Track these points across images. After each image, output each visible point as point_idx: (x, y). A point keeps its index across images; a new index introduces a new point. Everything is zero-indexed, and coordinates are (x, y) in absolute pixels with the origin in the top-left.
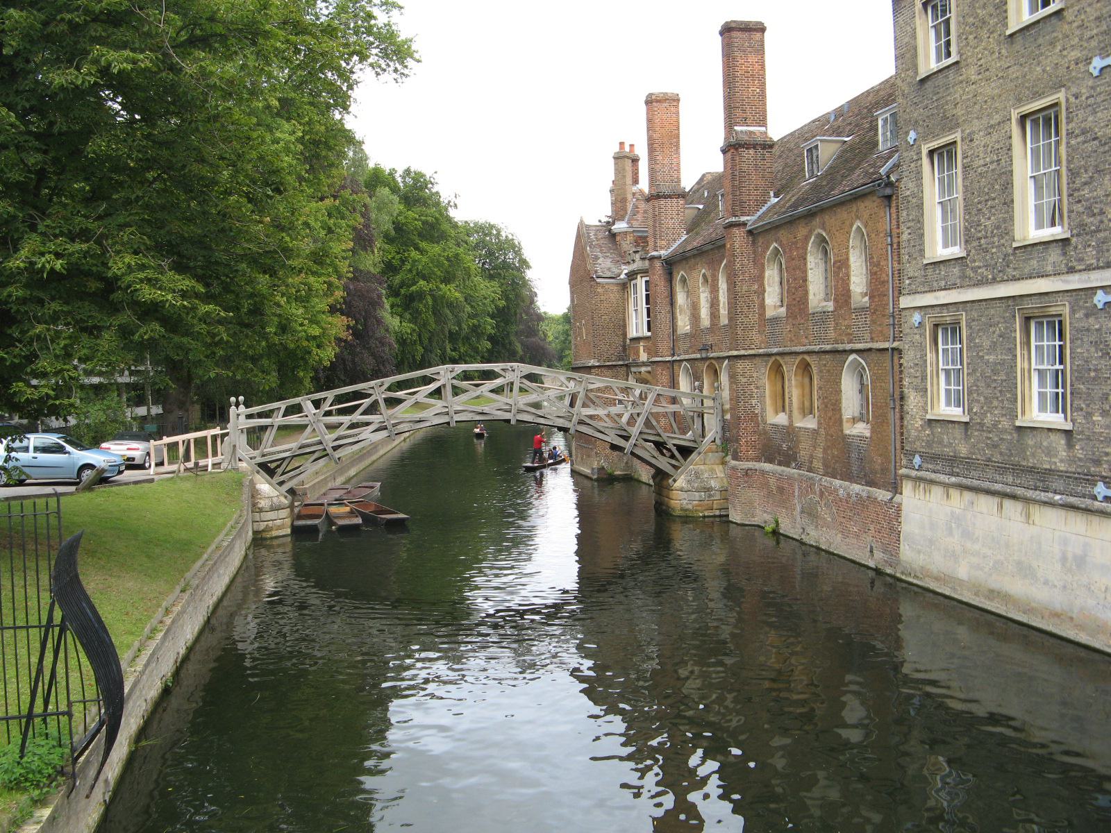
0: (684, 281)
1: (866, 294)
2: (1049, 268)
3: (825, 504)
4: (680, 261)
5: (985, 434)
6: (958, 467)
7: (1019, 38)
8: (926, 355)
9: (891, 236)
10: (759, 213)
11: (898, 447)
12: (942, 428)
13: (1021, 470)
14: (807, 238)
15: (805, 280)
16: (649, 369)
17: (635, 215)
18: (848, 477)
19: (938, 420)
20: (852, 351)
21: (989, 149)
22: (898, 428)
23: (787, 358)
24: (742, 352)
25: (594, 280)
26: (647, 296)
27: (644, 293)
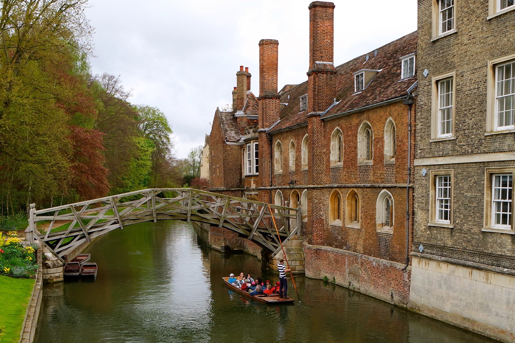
0: (279, 145)
1: (393, 157)
2: (506, 148)
3: (364, 270)
4: (277, 134)
5: (463, 235)
6: (446, 252)
7: (494, 22)
8: (429, 191)
9: (411, 126)
10: (327, 110)
11: (410, 238)
12: (436, 230)
13: (484, 255)
14: (358, 125)
15: (356, 148)
16: (257, 193)
18: (380, 256)
19: (435, 227)
20: (384, 188)
21: (473, 81)
22: (410, 230)
23: (343, 190)
24: (316, 186)
25: (225, 143)
26: (257, 153)
27: (255, 151)
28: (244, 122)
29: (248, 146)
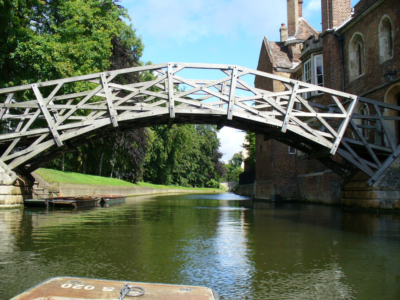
17: (301, 33)
28: (296, 49)
29: (306, 65)
